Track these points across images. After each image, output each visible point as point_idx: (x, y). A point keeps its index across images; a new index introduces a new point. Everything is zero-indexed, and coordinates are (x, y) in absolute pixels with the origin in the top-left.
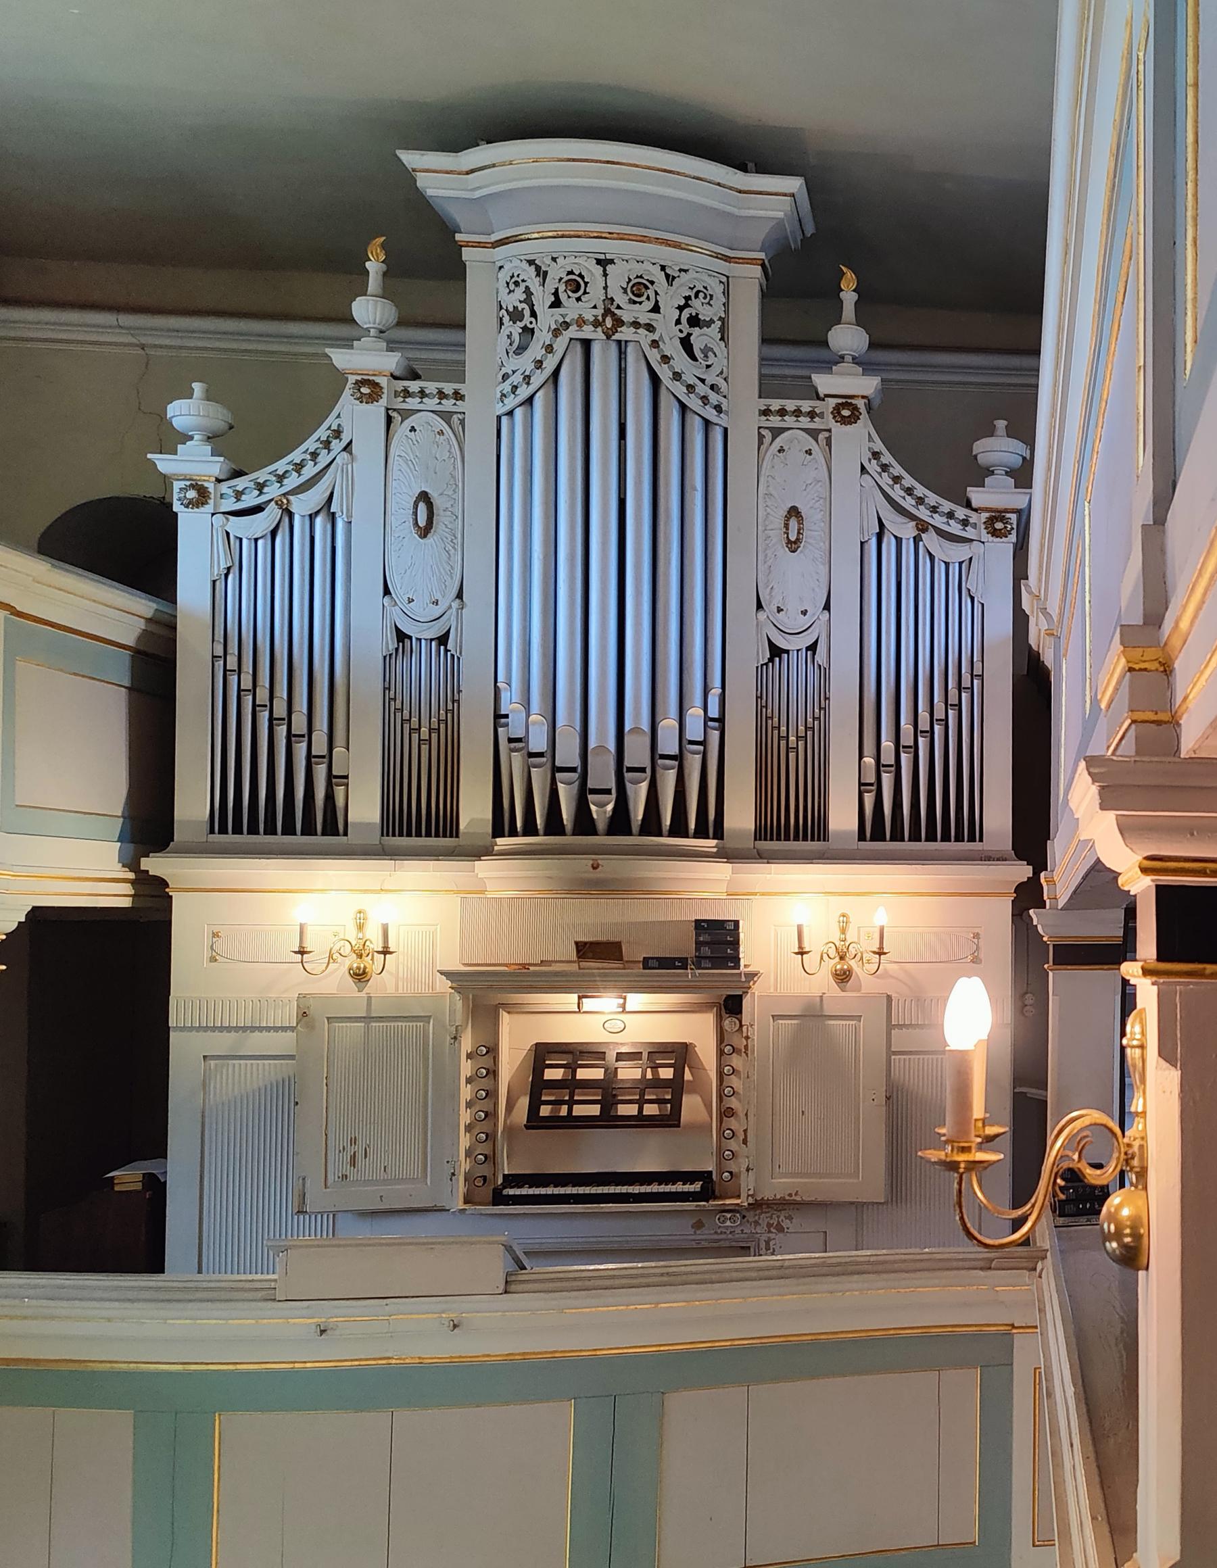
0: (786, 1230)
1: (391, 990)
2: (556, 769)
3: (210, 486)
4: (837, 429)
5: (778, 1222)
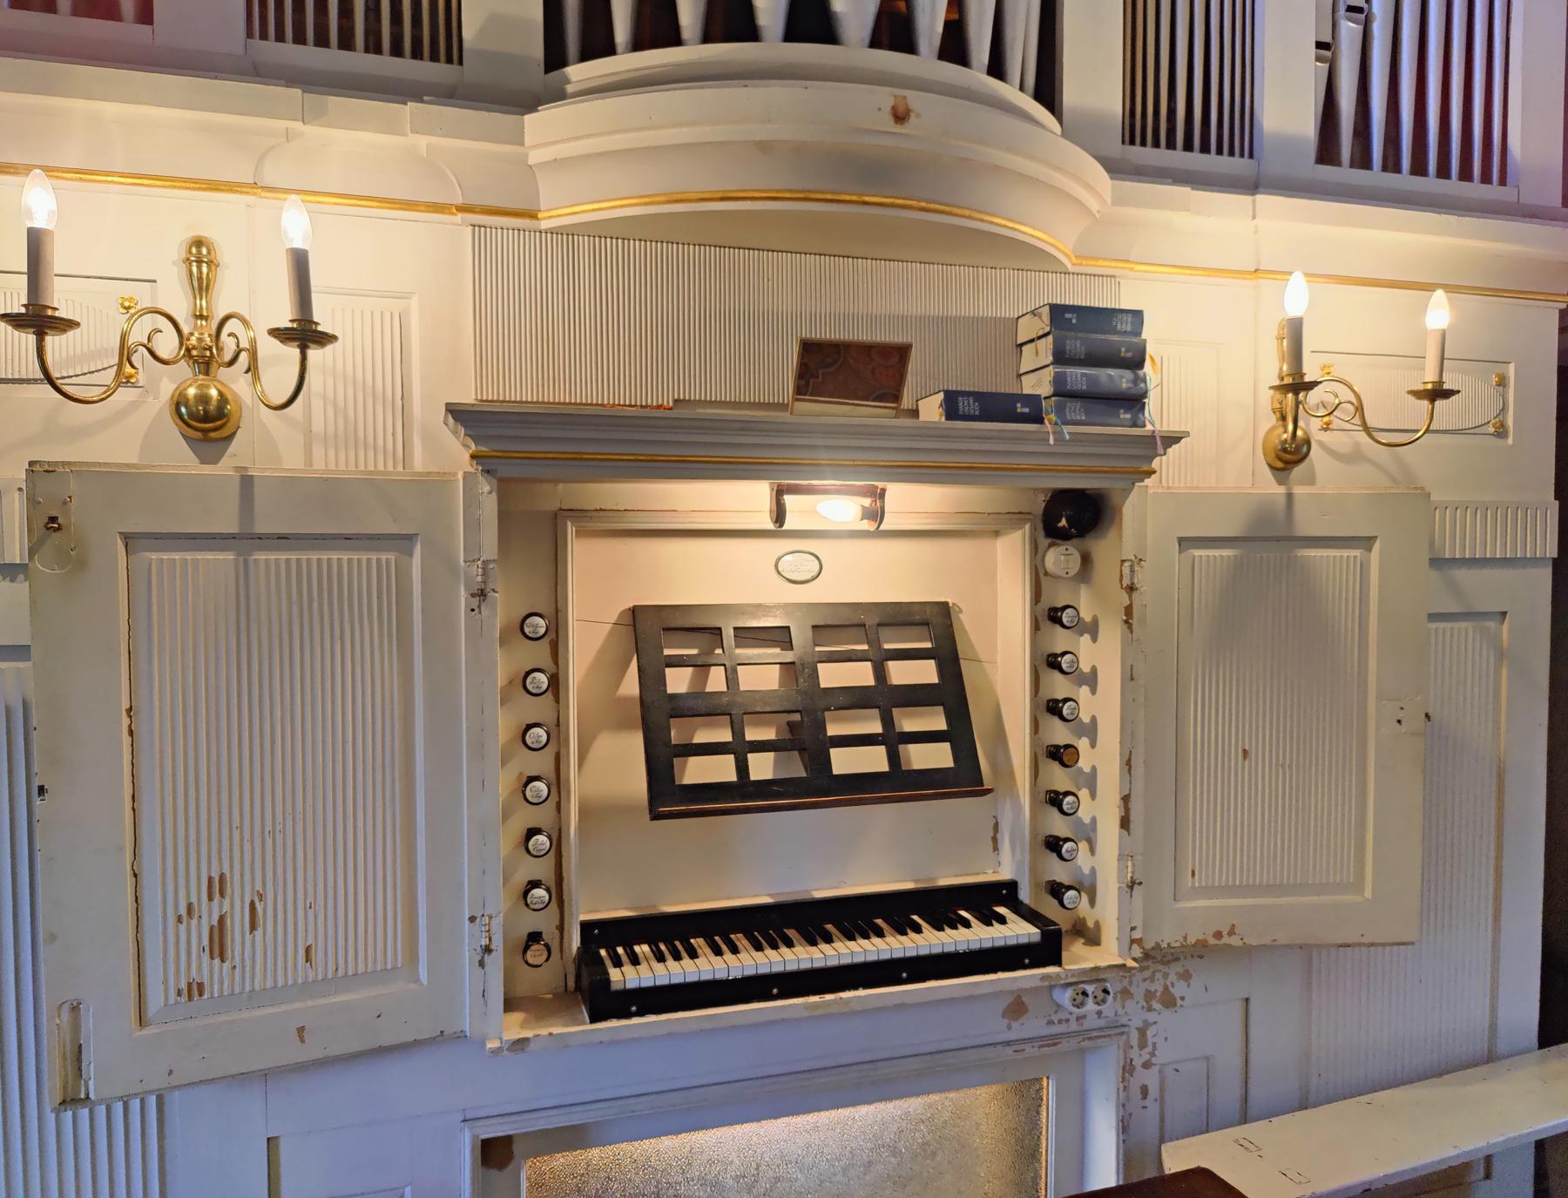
0: (1179, 1002)
1: (292, 460)
5: (1166, 988)
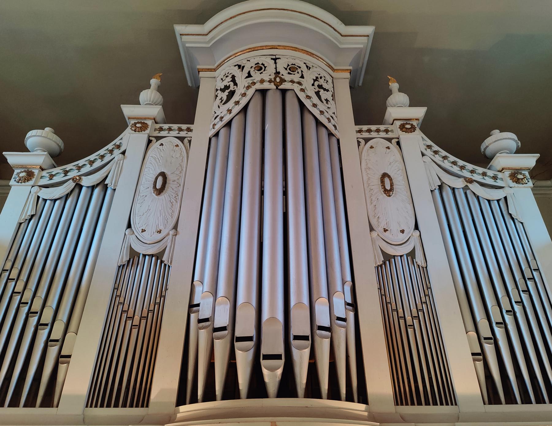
2: (235, 339)
3: (36, 172)
4: (404, 137)
